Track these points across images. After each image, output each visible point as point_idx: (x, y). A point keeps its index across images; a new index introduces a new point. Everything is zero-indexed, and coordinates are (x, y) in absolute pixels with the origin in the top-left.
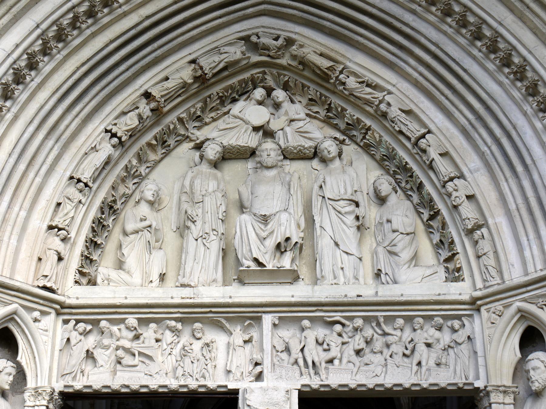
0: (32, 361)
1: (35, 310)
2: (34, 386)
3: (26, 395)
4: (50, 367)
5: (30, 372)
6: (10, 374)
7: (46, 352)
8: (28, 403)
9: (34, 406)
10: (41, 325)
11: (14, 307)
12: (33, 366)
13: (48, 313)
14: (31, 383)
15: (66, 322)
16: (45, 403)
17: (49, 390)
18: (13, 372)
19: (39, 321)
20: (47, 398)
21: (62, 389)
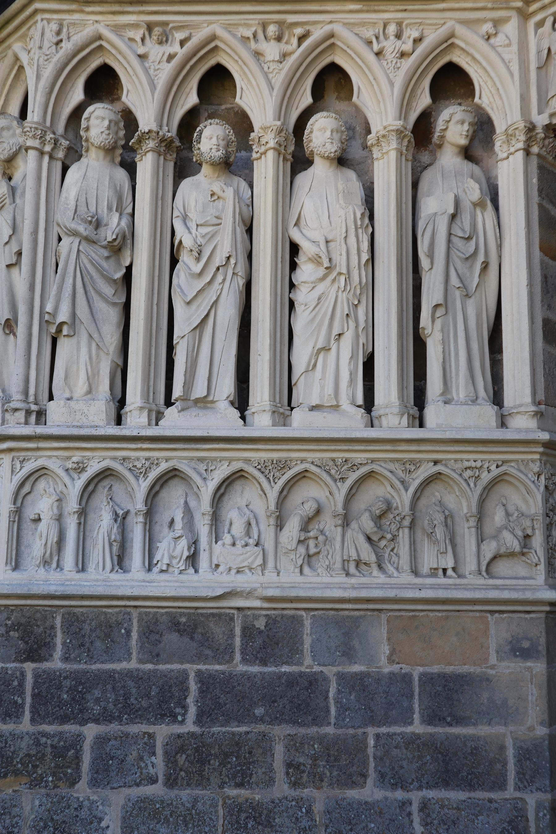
0: (497, 97)
1: (485, 21)
2: (504, 128)
3: (497, 144)
4: (522, 96)
5: (497, 113)
6: (463, 123)
7: (512, 74)
8: (502, 155)
9: (508, 157)
10: (498, 40)
11: (449, 24)
12: (499, 102)
13: (506, 20)
14: (500, 126)
15: (540, 24)
16: (521, 145)
17: (521, 125)
18: (469, 118)
19: (496, 34)
20: (523, 138)
21: (547, 122)
